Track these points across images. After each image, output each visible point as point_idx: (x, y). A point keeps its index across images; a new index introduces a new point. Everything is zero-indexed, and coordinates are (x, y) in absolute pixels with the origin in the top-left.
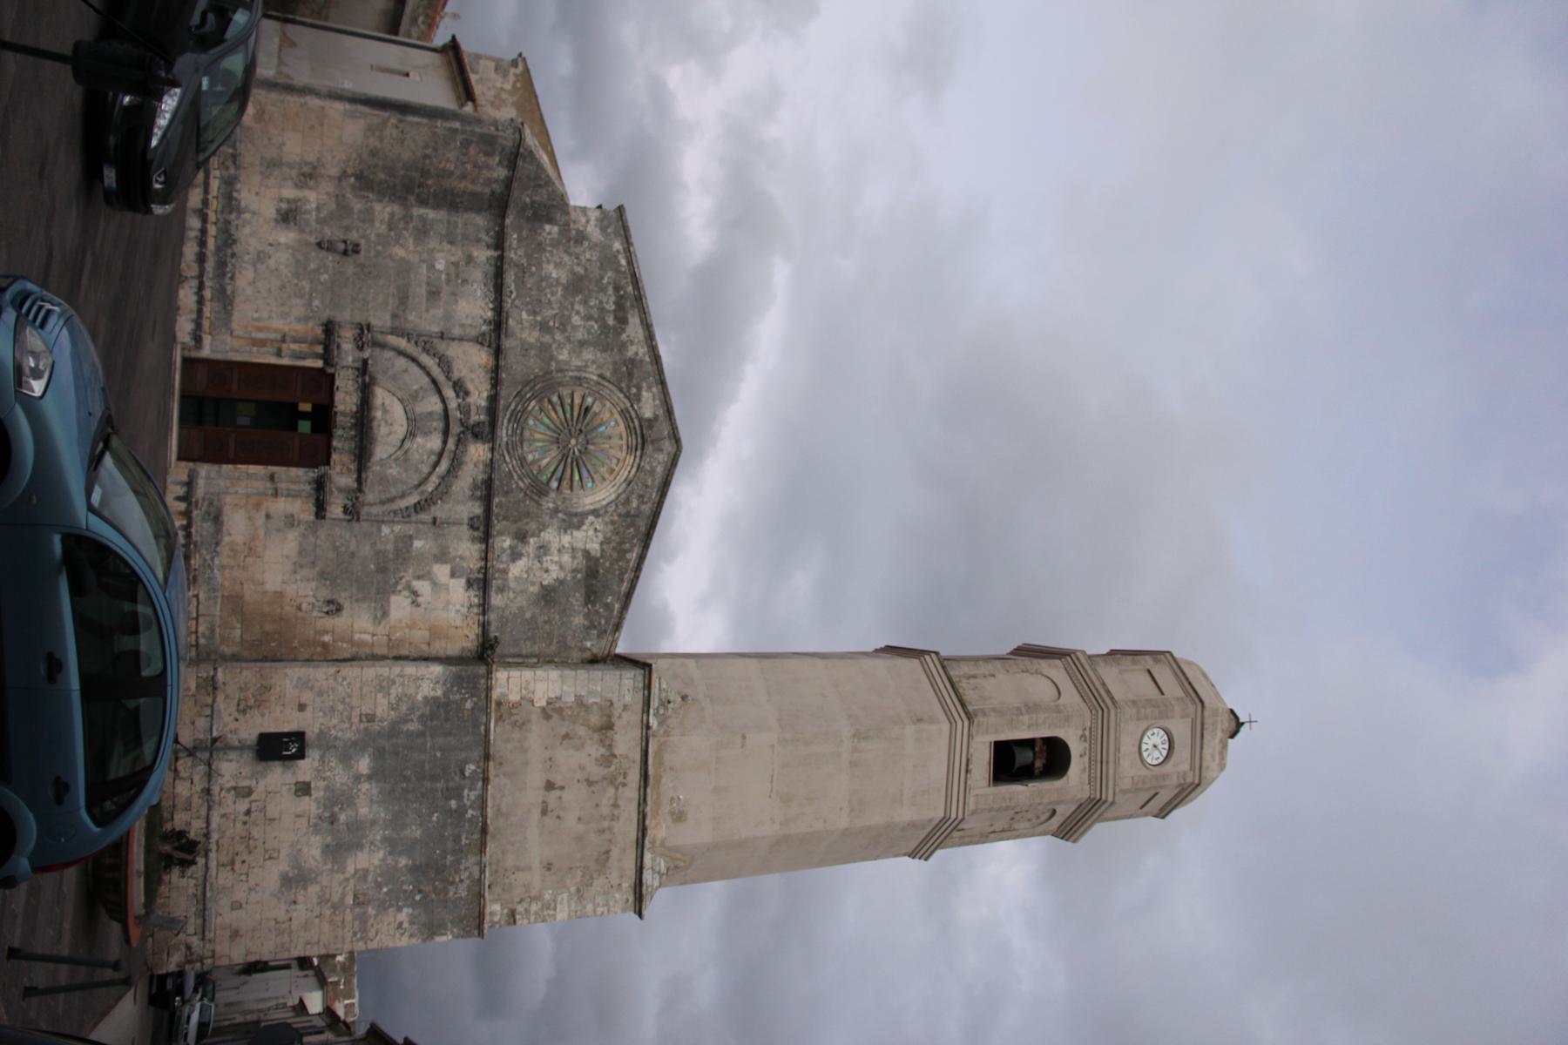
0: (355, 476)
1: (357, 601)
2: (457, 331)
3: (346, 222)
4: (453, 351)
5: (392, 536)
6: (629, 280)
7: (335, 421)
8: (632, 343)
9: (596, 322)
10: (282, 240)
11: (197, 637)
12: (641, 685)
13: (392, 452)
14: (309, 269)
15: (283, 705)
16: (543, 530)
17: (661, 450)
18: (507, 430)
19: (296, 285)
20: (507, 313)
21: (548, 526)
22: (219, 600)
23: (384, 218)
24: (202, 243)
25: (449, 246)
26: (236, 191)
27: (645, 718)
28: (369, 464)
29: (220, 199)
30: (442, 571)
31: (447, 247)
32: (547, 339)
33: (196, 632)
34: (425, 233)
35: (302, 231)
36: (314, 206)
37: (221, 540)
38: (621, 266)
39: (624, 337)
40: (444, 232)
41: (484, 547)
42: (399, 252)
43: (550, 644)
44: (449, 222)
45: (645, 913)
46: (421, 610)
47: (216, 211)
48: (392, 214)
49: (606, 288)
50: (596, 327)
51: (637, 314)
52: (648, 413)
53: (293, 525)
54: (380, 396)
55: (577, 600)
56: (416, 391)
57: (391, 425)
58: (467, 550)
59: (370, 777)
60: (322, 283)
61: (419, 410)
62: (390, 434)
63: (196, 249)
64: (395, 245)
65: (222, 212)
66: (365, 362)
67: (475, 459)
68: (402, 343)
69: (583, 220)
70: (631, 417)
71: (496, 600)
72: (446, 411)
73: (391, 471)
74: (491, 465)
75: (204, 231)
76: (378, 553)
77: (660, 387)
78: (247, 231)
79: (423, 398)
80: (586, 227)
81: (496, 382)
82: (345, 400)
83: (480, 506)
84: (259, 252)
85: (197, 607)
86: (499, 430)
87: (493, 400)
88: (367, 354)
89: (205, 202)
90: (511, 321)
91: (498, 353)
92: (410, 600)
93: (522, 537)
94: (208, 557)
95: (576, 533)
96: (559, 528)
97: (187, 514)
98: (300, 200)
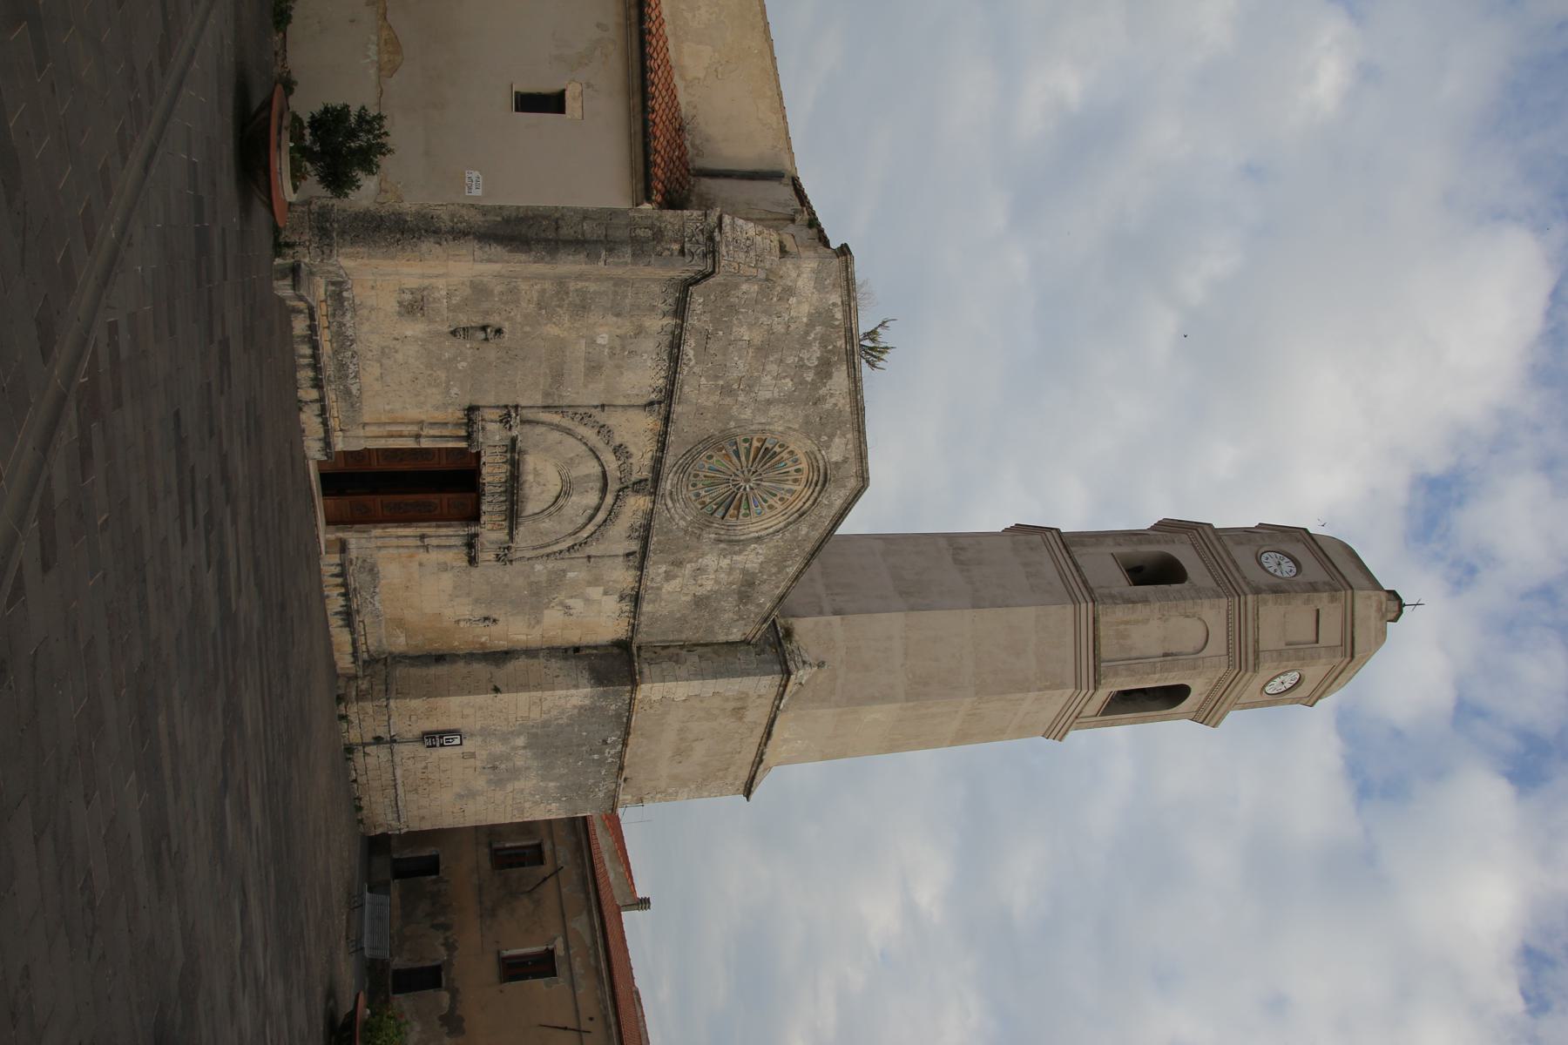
0: (507, 531)
1: (511, 615)
2: (621, 401)
3: (486, 305)
4: (613, 419)
5: (545, 571)
6: (842, 333)
7: (483, 490)
8: (832, 395)
9: (792, 380)
10: (409, 333)
11: (367, 646)
12: (778, 683)
13: (545, 507)
14: (443, 358)
15: (449, 716)
16: (701, 557)
17: (845, 486)
18: (672, 480)
19: (430, 375)
20: (682, 381)
21: (707, 554)
22: (383, 625)
23: (532, 297)
24: (316, 366)
25: (615, 319)
26: (346, 290)
27: (777, 703)
28: (520, 520)
29: (329, 302)
30: (595, 593)
31: (611, 319)
32: (728, 400)
33: (366, 643)
34: (584, 307)
35: (431, 321)
36: (444, 293)
37: (379, 582)
38: (837, 320)
39: (823, 391)
40: (609, 305)
41: (639, 573)
42: (552, 330)
43: (698, 632)
44: (616, 293)
45: (753, 797)
46: (574, 617)
47: (327, 316)
48: (543, 291)
49: (810, 344)
50: (790, 384)
51: (845, 367)
52: (836, 457)
53: (447, 570)
54: (531, 462)
55: (729, 604)
56: (571, 459)
57: (544, 485)
58: (624, 577)
59: (524, 748)
60: (460, 371)
61: (574, 474)
62: (543, 492)
63: (311, 374)
64: (546, 324)
65: (334, 315)
66: (514, 440)
67: (634, 508)
68: (556, 418)
69: (794, 274)
70: (815, 458)
71: (646, 608)
72: (604, 474)
73: (544, 525)
74: (650, 515)
75: (315, 357)
76: (531, 584)
77: (856, 433)
78: (366, 328)
79: (579, 463)
80: (795, 281)
81: (662, 446)
82: (493, 472)
83: (637, 545)
84: (383, 348)
85: (364, 628)
86: (663, 483)
87: (658, 463)
88: (515, 432)
89: (313, 328)
90: (686, 389)
91: (667, 420)
92: (563, 612)
93: (679, 564)
94: (368, 597)
95: (735, 557)
96: (719, 555)
97: (342, 574)
98: (424, 289)
